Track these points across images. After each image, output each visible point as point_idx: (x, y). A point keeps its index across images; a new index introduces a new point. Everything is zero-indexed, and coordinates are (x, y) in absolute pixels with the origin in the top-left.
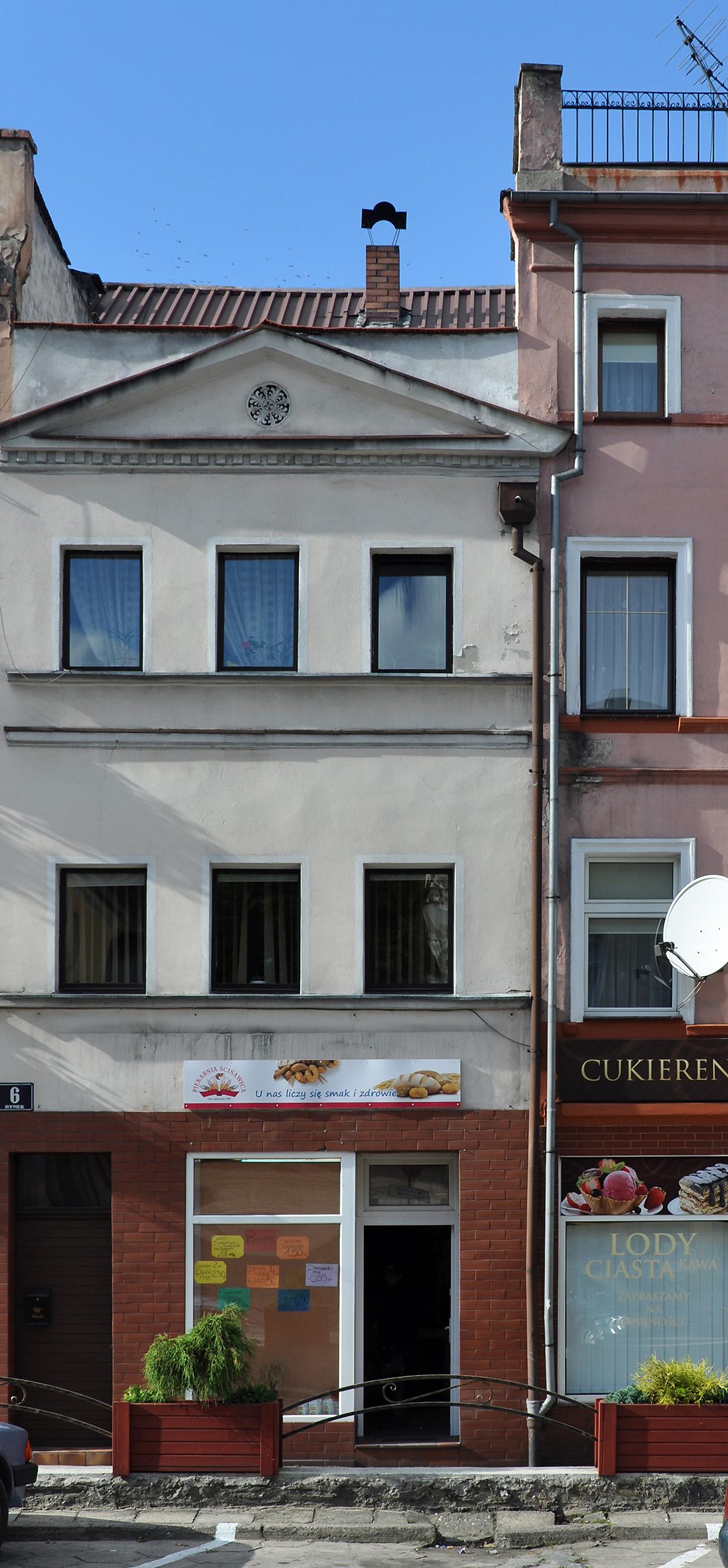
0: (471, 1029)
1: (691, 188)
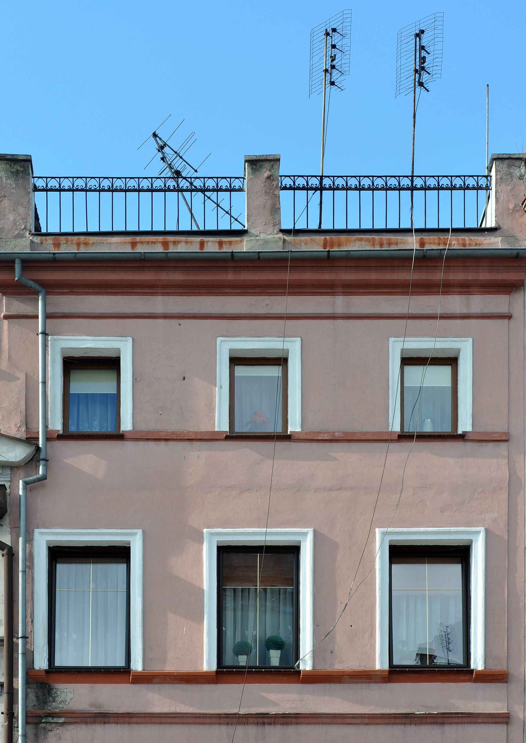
1: (141, 249)
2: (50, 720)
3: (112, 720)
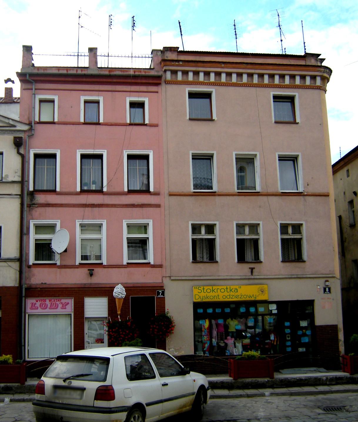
0: (5, 266)
2: (34, 206)
3: (51, 206)
